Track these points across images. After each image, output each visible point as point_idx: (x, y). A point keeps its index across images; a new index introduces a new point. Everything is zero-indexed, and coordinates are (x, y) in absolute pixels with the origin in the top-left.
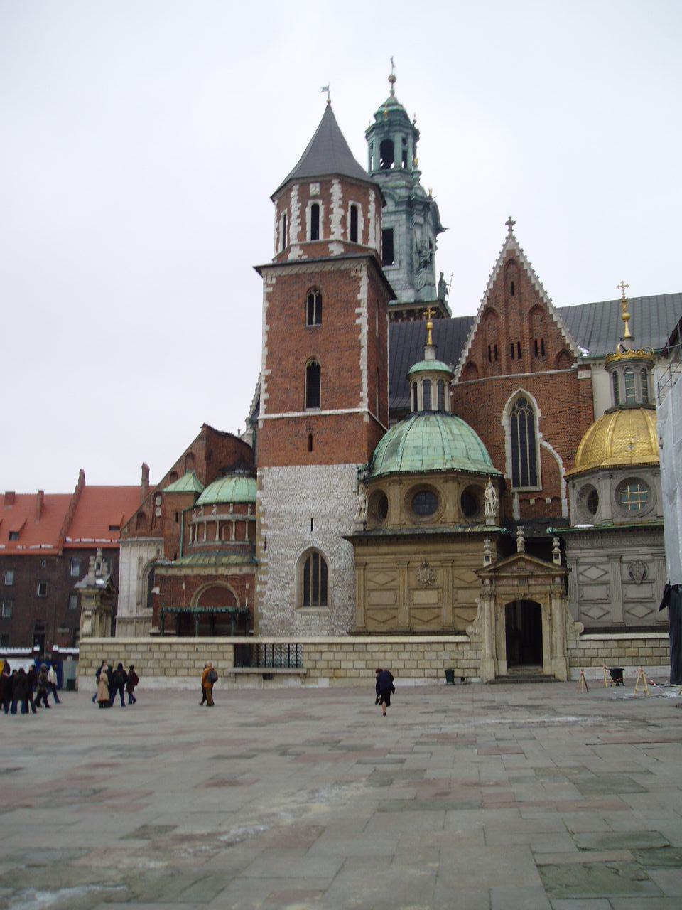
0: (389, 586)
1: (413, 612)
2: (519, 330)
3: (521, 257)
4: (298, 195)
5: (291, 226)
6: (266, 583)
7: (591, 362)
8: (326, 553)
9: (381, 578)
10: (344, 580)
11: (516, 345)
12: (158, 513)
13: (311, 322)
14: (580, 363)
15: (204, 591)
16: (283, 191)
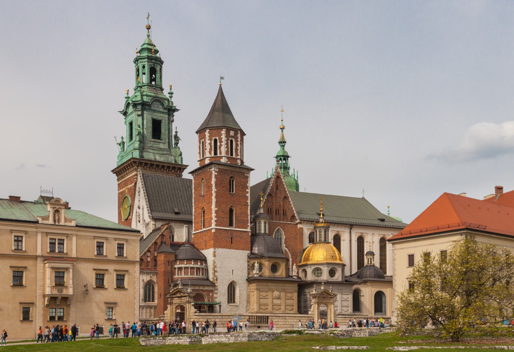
0: (265, 297)
1: (274, 307)
2: (279, 204)
6: (217, 294)
7: (302, 222)
11: (277, 210)
12: (149, 259)
13: (230, 191)
14: (298, 221)
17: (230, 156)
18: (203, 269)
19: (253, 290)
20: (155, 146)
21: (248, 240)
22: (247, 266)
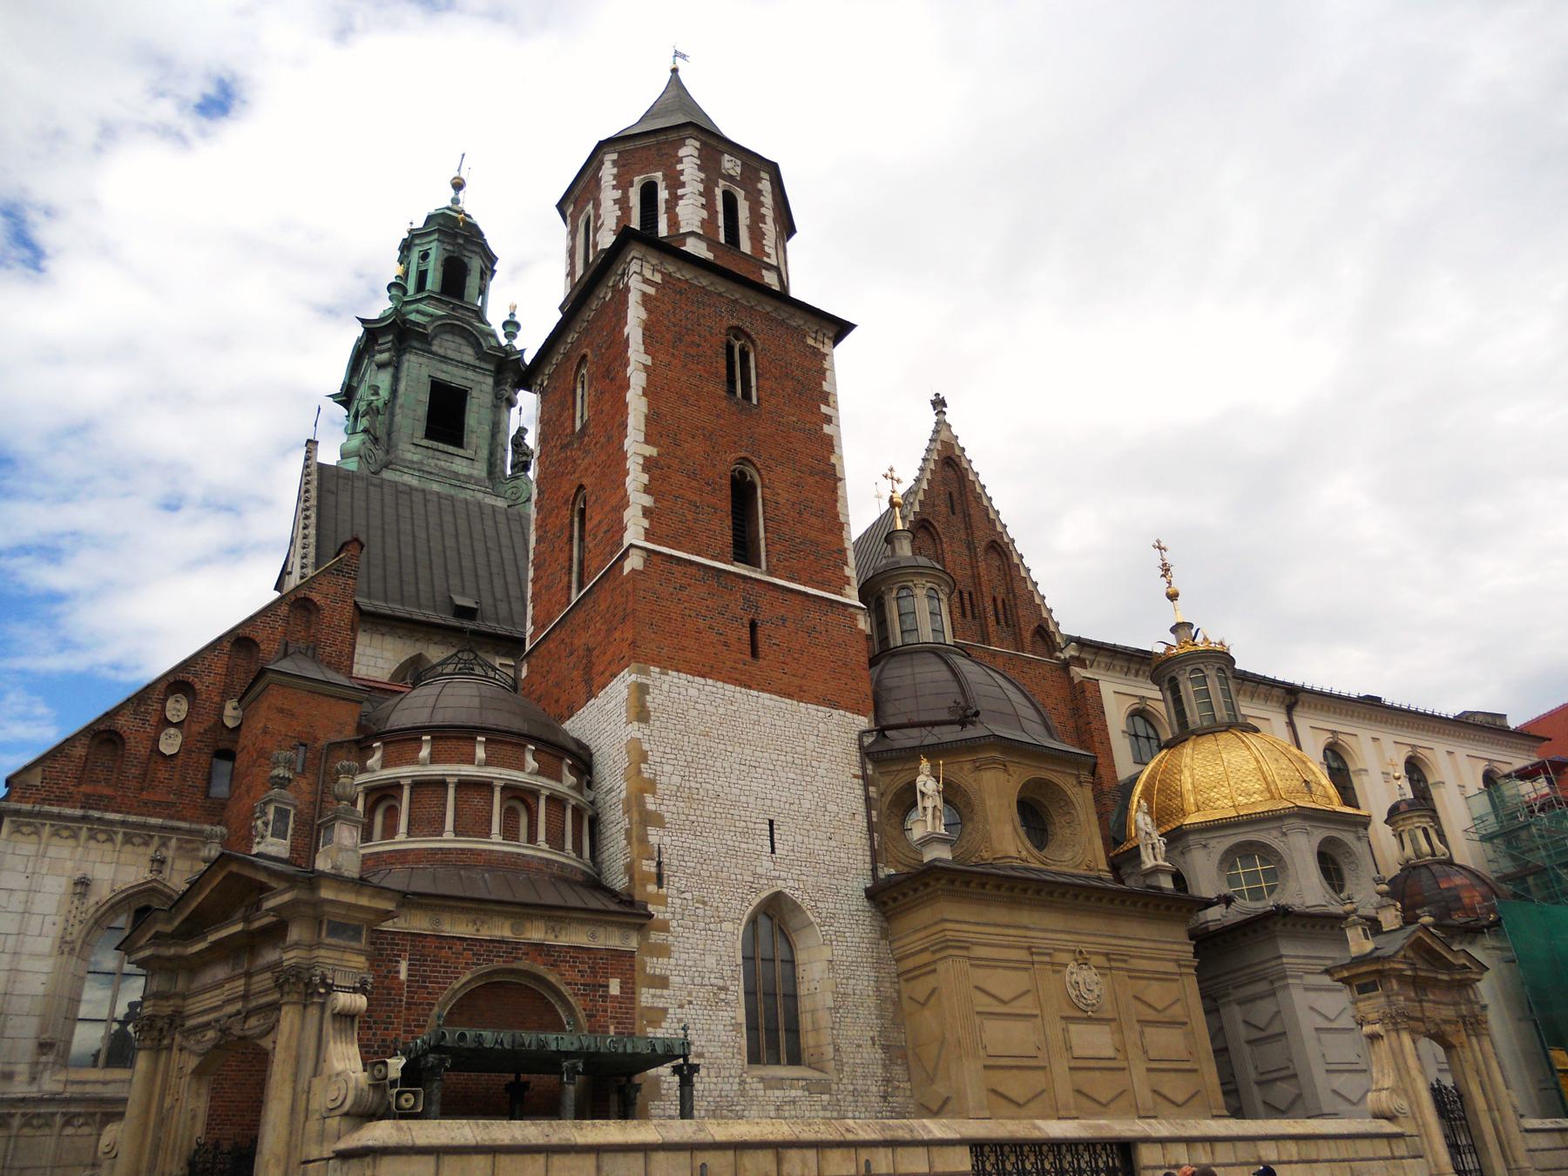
0: (1016, 1008)
2: (969, 572)
3: (963, 458)
4: (699, 157)
5: (680, 202)
6: (662, 982)
8: (808, 913)
9: (1004, 983)
10: (854, 994)
11: (966, 596)
14: (1071, 651)
15: (459, 995)
16: (652, 140)
17: (722, 241)
18: (556, 801)
19: (925, 957)
20: (433, 462)
21: (852, 651)
22: (862, 809)
